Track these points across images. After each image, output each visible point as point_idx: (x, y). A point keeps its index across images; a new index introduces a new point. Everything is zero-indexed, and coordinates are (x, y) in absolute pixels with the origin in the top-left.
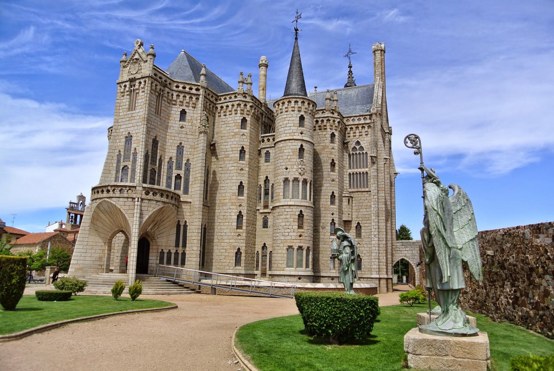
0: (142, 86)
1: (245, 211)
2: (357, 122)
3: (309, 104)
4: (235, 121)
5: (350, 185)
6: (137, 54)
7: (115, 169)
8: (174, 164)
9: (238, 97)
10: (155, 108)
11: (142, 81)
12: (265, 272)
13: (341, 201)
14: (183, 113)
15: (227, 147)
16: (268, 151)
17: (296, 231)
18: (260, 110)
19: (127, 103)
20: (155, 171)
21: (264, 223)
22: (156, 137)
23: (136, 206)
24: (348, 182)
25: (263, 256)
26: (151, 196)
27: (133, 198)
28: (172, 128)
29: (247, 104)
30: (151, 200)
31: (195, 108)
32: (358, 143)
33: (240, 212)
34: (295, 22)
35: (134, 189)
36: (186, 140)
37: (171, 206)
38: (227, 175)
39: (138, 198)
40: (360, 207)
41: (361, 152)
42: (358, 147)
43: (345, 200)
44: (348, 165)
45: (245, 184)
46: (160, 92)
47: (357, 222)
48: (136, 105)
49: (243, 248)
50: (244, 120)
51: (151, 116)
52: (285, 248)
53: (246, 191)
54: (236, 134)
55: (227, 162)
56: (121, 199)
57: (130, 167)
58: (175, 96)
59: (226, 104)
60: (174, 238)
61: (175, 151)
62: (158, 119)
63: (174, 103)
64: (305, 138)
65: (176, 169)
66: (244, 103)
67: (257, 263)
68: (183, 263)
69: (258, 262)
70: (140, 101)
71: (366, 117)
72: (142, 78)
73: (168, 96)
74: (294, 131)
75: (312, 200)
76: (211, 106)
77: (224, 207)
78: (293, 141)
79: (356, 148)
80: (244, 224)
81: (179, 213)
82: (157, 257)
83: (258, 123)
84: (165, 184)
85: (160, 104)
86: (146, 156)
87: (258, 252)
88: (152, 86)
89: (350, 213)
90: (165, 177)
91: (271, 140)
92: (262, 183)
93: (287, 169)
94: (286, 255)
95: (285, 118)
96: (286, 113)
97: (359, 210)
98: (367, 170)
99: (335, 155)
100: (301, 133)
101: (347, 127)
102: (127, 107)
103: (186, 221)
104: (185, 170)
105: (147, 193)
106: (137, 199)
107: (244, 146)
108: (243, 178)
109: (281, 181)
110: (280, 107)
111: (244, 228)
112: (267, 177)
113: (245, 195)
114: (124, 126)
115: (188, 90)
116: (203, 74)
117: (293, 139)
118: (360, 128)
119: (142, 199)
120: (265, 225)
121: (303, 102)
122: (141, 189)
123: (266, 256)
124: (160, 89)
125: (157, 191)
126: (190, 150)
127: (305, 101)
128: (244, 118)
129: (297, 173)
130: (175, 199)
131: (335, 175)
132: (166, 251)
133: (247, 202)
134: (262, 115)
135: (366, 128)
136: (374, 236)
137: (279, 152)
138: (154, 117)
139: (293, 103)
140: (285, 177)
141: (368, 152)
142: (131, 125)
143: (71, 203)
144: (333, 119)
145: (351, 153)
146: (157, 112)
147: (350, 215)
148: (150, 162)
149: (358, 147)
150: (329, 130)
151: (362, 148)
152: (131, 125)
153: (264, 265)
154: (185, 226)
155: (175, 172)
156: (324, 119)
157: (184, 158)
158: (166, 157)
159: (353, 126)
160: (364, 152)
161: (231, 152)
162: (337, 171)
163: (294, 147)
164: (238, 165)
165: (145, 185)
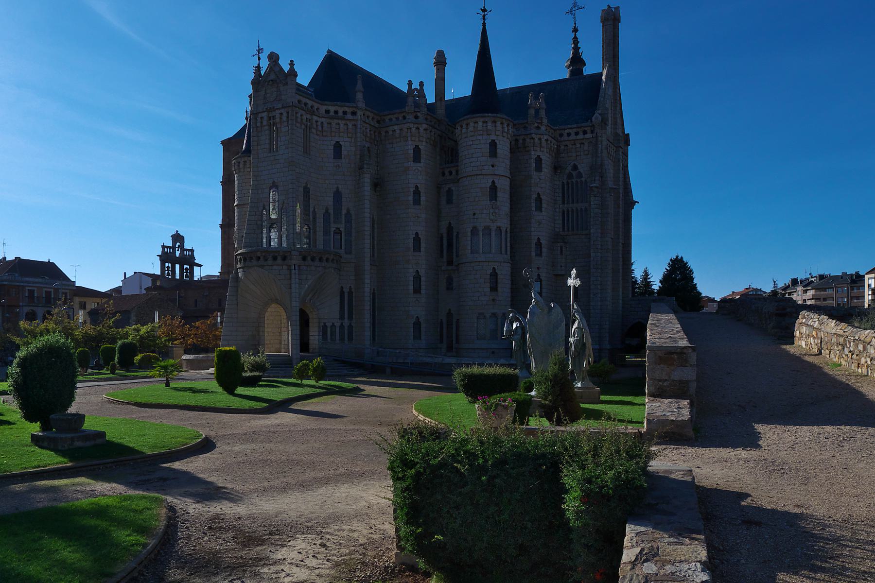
2: (573, 137)
3: (502, 123)
5: (564, 226)
9: (407, 117)
10: (302, 146)
11: (282, 111)
14: (338, 147)
23: (293, 276)
24: (561, 222)
29: (419, 126)
31: (351, 138)
32: (575, 168)
37: (333, 271)
39: (295, 265)
41: (579, 180)
42: (574, 173)
44: (561, 199)
50: (417, 150)
58: (325, 125)
59: (391, 128)
61: (332, 199)
63: (324, 134)
64: (497, 172)
66: (416, 126)
68: (351, 338)
72: (283, 107)
75: (509, 253)
85: (308, 139)
87: (441, 320)
91: (454, 173)
92: (444, 231)
93: (474, 214)
100: (493, 166)
102: (268, 146)
103: (350, 287)
104: (345, 222)
105: (304, 259)
107: (418, 185)
110: (464, 130)
111: (423, 292)
113: (423, 249)
115: (342, 114)
117: (481, 174)
118: (578, 145)
119: (299, 266)
120: (449, 287)
121: (495, 122)
128: (417, 146)
130: (337, 261)
132: (329, 325)
135: (586, 144)
139: (480, 124)
143: (164, 247)
144: (538, 136)
145: (565, 182)
149: (574, 173)
150: (533, 153)
151: (580, 175)
154: (350, 293)
157: (343, 208)
159: (566, 143)
160: (583, 179)
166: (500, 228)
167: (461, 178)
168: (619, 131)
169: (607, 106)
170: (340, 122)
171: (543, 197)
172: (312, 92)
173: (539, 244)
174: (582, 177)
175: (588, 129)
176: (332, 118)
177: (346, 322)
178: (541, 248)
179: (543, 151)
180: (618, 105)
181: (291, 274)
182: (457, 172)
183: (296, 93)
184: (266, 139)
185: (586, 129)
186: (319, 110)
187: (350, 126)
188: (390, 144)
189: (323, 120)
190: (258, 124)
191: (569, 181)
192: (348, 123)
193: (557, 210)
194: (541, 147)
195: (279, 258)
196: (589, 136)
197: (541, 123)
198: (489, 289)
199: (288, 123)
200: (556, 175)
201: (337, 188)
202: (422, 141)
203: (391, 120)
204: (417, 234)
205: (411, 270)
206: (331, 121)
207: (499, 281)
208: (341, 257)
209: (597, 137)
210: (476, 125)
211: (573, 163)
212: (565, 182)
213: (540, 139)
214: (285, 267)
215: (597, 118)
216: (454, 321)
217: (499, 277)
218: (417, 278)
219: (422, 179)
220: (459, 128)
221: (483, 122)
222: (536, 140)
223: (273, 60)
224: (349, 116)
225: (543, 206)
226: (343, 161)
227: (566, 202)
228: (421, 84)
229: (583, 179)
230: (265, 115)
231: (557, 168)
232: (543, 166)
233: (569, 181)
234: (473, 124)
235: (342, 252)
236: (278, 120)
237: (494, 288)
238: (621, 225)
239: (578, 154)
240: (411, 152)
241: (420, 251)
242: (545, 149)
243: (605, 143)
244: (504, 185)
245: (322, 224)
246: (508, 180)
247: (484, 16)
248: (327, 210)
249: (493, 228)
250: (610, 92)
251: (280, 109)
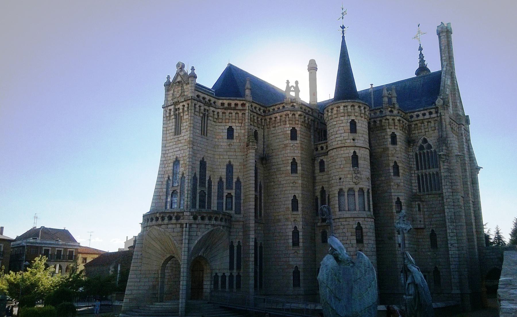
0: (186, 109)
2: (421, 117)
3: (359, 107)
4: (284, 133)
6: (179, 77)
7: (165, 193)
8: (225, 184)
9: (286, 107)
11: (184, 103)
14: (230, 132)
15: (278, 160)
17: (355, 245)
18: (311, 117)
19: (174, 127)
20: (205, 193)
22: (203, 158)
23: (184, 232)
24: (417, 184)
26: (199, 220)
27: (182, 225)
28: (219, 147)
29: (295, 113)
30: (199, 224)
31: (242, 123)
32: (425, 141)
33: (296, 227)
34: (341, 19)
35: (182, 214)
36: (234, 157)
37: (221, 228)
38: (279, 189)
39: (186, 224)
40: (433, 213)
41: (429, 151)
44: (415, 166)
46: (204, 112)
47: (431, 229)
48: (182, 128)
51: (197, 138)
54: (286, 146)
55: (278, 176)
56: (170, 226)
57: (178, 191)
58: (221, 114)
59: (274, 115)
60: (228, 259)
61: (225, 170)
62: (205, 140)
63: (220, 121)
65: (227, 189)
66: (292, 113)
68: (239, 286)
70: (185, 124)
71: (432, 110)
72: (185, 101)
73: (214, 115)
74: (346, 138)
75: (372, 210)
76: (259, 119)
77: (279, 224)
78: (345, 148)
79: (423, 147)
81: (232, 234)
82: (211, 281)
83: (310, 131)
84: (216, 205)
85: (206, 124)
86: (195, 178)
88: (195, 108)
90: (216, 198)
92: (318, 194)
93: (340, 179)
95: (335, 125)
96: (335, 120)
98: (438, 169)
100: (354, 140)
101: (412, 123)
102: (173, 131)
104: (236, 189)
105: (195, 218)
106: (185, 225)
107: (295, 158)
108: (297, 192)
109: (336, 192)
110: (330, 114)
111: (301, 244)
112: (323, 188)
114: (172, 151)
116: (248, 89)
117: (345, 147)
118: (426, 124)
119: (190, 225)
122: (188, 214)
124: (205, 109)
125: (205, 215)
126: (240, 167)
127: (354, 104)
128: (294, 128)
129: (352, 183)
130: (226, 220)
133: (302, 216)
134: (314, 121)
135: (433, 122)
136: (451, 245)
137: (331, 161)
138: (200, 139)
139: (342, 108)
140: (339, 187)
141: (437, 150)
142: (177, 149)
144: (392, 117)
145: (418, 152)
146: (203, 133)
147: (422, 222)
148: (198, 184)
149: (425, 146)
150: (388, 130)
151: (430, 147)
152: (177, 149)
155: (226, 192)
156: (381, 118)
157: (234, 177)
158: (216, 177)
159: (417, 122)
160: (433, 150)
161: (283, 166)
163: (347, 155)
164: (291, 178)
165: (193, 210)
166: (362, 189)
167: (328, 151)
168: (461, 113)
169: (447, 93)
170: (232, 111)
171: (400, 165)
172: (214, 92)
173: (399, 202)
174: (432, 148)
175: (433, 111)
176: (225, 109)
177: (235, 272)
178: (401, 206)
179: (397, 129)
180: (457, 93)
181: (183, 231)
182: (327, 146)
183: (196, 90)
184: (173, 125)
185: (432, 110)
186: (216, 104)
187: (240, 114)
188: (273, 127)
189: (219, 110)
190: (168, 115)
191: (421, 152)
192: (239, 112)
193: (413, 175)
194: (395, 125)
195: (174, 218)
196: (434, 115)
197: (394, 108)
198: (355, 241)
199: (188, 113)
200: (410, 147)
201: (230, 162)
202: (298, 124)
203: (274, 109)
204: (295, 196)
205: (290, 227)
206: (226, 111)
207: (364, 234)
208: (231, 217)
209: (441, 116)
210: (339, 109)
211: (423, 137)
212: (418, 152)
213: (393, 120)
214: (178, 226)
215: (439, 102)
217: (364, 230)
218: (296, 233)
219: (298, 153)
220: (326, 113)
221: (344, 107)
222: (391, 121)
223: (180, 67)
224: (240, 107)
225: (400, 172)
226: (235, 141)
227: (420, 168)
228: (297, 83)
229: (433, 150)
230: (173, 107)
231: (410, 142)
232: (398, 140)
233: (421, 152)
234: (337, 108)
235: (233, 212)
236: (181, 111)
237: (360, 241)
238: (469, 186)
239: (427, 130)
240: (289, 132)
241: (297, 210)
242: (399, 128)
243: (448, 120)
244: (364, 154)
245: (217, 190)
246: (368, 150)
247: (343, 31)
248: (221, 179)
249: (357, 190)
250: (449, 82)
251: (182, 102)
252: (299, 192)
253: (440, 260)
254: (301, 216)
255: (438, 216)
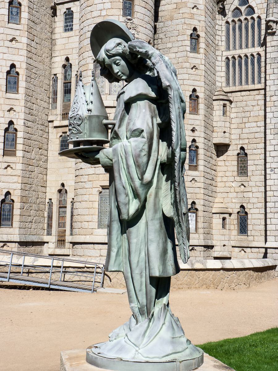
1: (21, 122)
12: (63, 239)
13: (209, 107)
16: (69, 9)
21: (62, 146)
24: (224, 74)
25: (60, 207)
33: (11, 123)
40: (245, 120)
43: (218, 106)
44: (224, 43)
45: (21, 69)
47: (239, 146)
49: (16, 191)
52: (95, 191)
53: (22, 84)
67: (48, 221)
69: (50, 218)
80: (20, 147)
89: (227, 130)
92: (59, 70)
94: (96, 205)
97: (243, 125)
99: (199, 21)
111: (19, 153)
112: (67, 59)
113: (22, 90)
123: (66, 207)
131: (198, 59)
136: (272, 171)
141: (263, 17)
145: (230, 20)
149: (243, 8)
151: (251, 10)
153: (61, 225)
162: (202, 51)
174: (254, 12)
216: (69, 201)
229: (255, 16)
233: (236, 19)
252: (24, 59)
253: (250, 195)
254: (22, 103)
255: (254, 124)
